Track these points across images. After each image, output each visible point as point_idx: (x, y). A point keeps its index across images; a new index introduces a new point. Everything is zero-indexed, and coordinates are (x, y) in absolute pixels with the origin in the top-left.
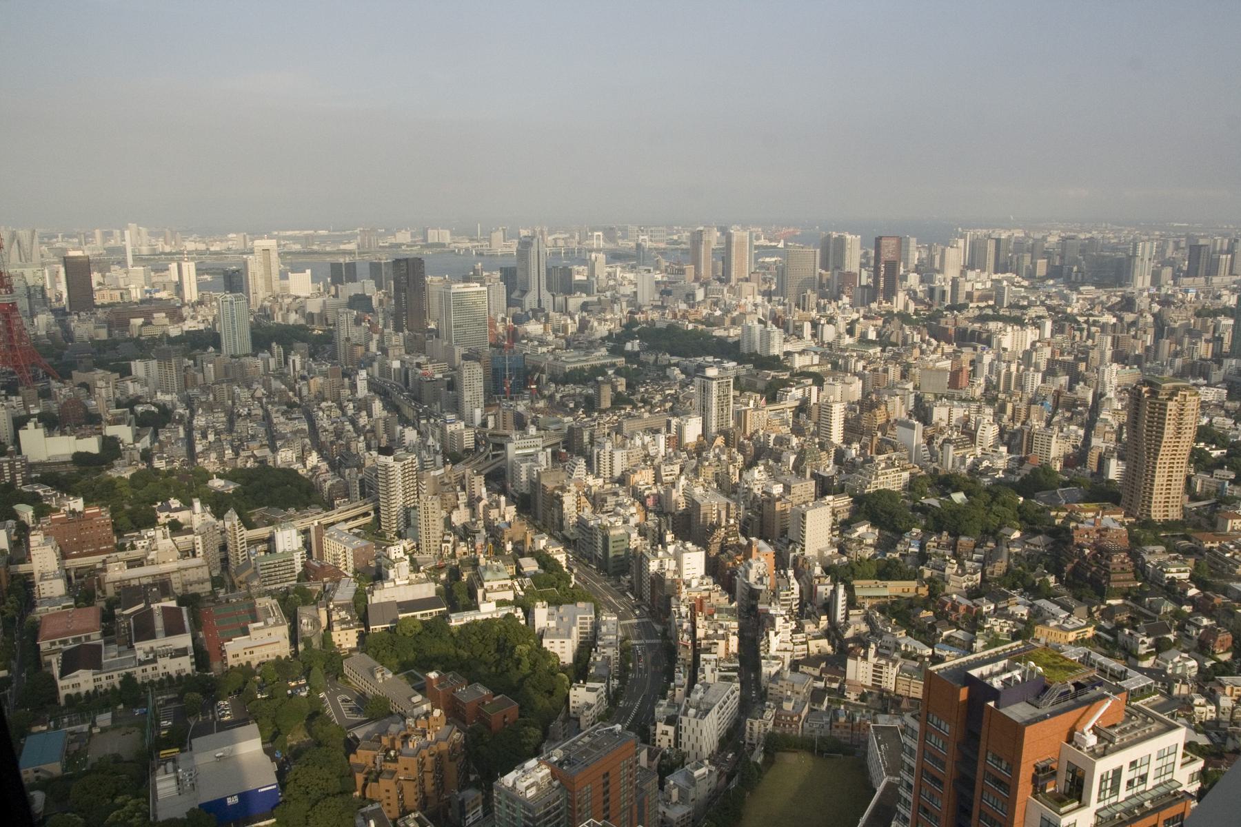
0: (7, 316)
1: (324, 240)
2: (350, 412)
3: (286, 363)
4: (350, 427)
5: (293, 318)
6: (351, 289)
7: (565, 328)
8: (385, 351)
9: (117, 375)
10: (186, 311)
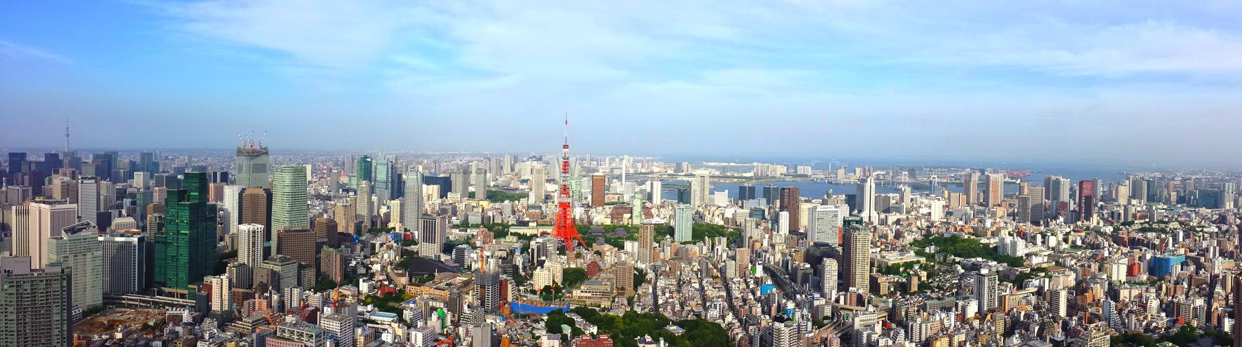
1: (732, 169)
2: (752, 286)
4: (751, 296)
6: (751, 204)
7: (886, 236)
8: (773, 246)
10: (654, 211)
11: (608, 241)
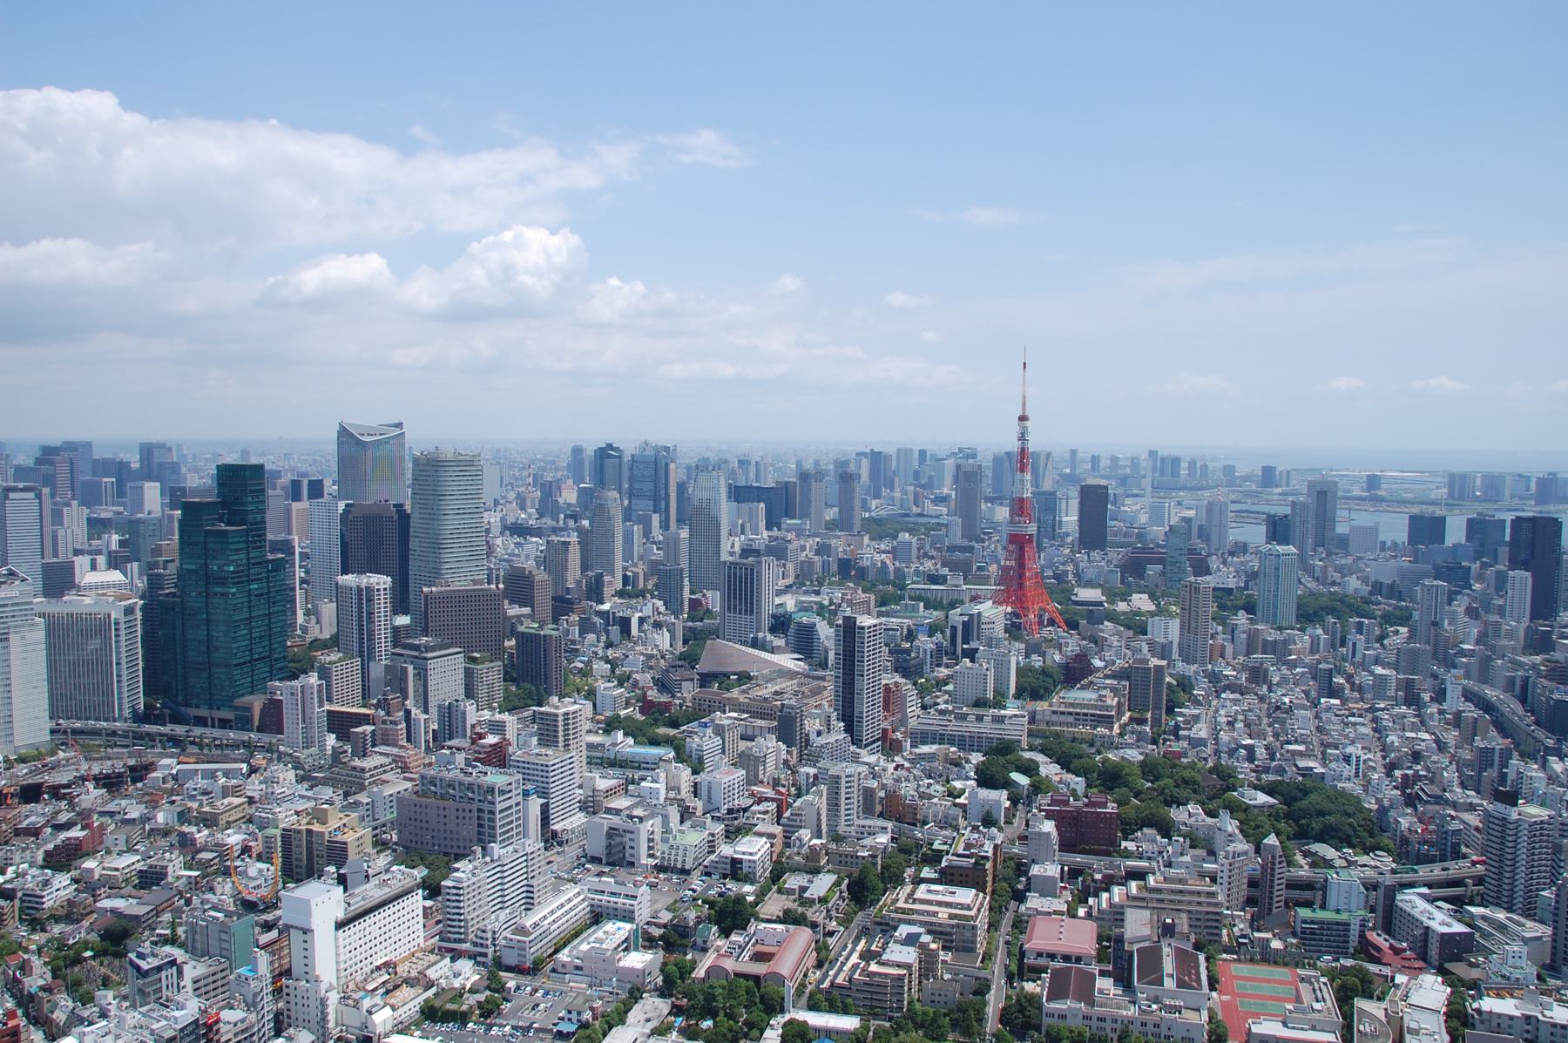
0: (1022, 549)
3: (1343, 644)
5: (1353, 584)
9: (1131, 633)
10: (1214, 563)
11: (1112, 617)
